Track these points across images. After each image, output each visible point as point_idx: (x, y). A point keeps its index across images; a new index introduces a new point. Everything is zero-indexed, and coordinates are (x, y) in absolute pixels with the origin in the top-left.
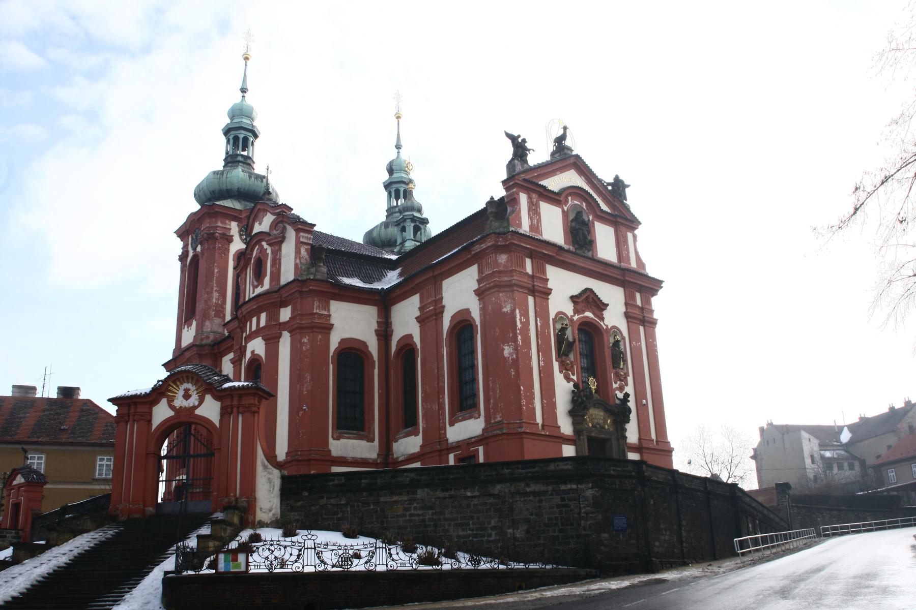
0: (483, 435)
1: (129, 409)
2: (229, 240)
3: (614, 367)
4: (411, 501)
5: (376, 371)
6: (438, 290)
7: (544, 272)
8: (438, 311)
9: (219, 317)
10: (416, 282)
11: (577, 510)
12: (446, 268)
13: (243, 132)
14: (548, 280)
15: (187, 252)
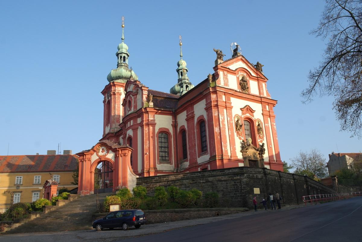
0: (209, 160)
1: (84, 157)
2: (120, 94)
3: (258, 134)
4: (181, 185)
5: (172, 139)
6: (193, 109)
7: (229, 100)
8: (193, 116)
9: (118, 122)
10: (185, 106)
11: (240, 187)
13: (123, 54)
14: (231, 103)
15: (106, 99)
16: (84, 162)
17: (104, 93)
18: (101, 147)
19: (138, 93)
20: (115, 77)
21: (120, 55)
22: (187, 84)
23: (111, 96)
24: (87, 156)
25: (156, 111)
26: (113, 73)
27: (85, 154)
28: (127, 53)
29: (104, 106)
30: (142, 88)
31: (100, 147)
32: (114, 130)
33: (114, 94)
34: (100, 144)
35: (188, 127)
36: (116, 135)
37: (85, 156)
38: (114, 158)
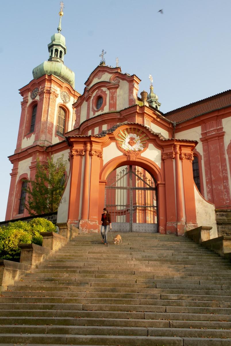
8: (221, 135)
10: (202, 119)
12: (225, 112)
13: (60, 47)
16: (88, 157)
17: (23, 91)
18: (129, 133)
19: (119, 86)
20: (49, 71)
21: (55, 48)
22: (157, 105)
23: (42, 94)
24: (95, 147)
25: (155, 117)
26: (48, 66)
27: (92, 139)
28: (66, 48)
29: (23, 110)
30: (134, 77)
31: (126, 133)
32: (44, 143)
33: (49, 92)
34: (128, 127)
35: (204, 150)
36: (47, 151)
37: (89, 145)
38: (160, 161)
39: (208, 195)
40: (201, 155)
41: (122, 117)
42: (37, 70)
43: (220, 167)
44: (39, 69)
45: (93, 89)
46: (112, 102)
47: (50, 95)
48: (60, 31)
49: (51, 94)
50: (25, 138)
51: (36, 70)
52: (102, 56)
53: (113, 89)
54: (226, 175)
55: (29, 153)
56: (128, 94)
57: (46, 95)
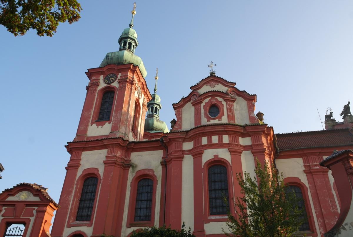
10: (305, 152)
20: (127, 61)
21: (129, 41)
36: (128, 147)
39: (320, 229)
40: (307, 186)
41: (245, 132)
42: (114, 56)
43: (330, 202)
44: (117, 56)
45: (206, 96)
46: (230, 114)
47: (132, 86)
48: (132, 27)
49: (133, 85)
50: (94, 125)
51: (113, 55)
52: (211, 65)
53: (230, 101)
54: (336, 211)
55: (104, 144)
56: (247, 111)
57: (128, 85)
